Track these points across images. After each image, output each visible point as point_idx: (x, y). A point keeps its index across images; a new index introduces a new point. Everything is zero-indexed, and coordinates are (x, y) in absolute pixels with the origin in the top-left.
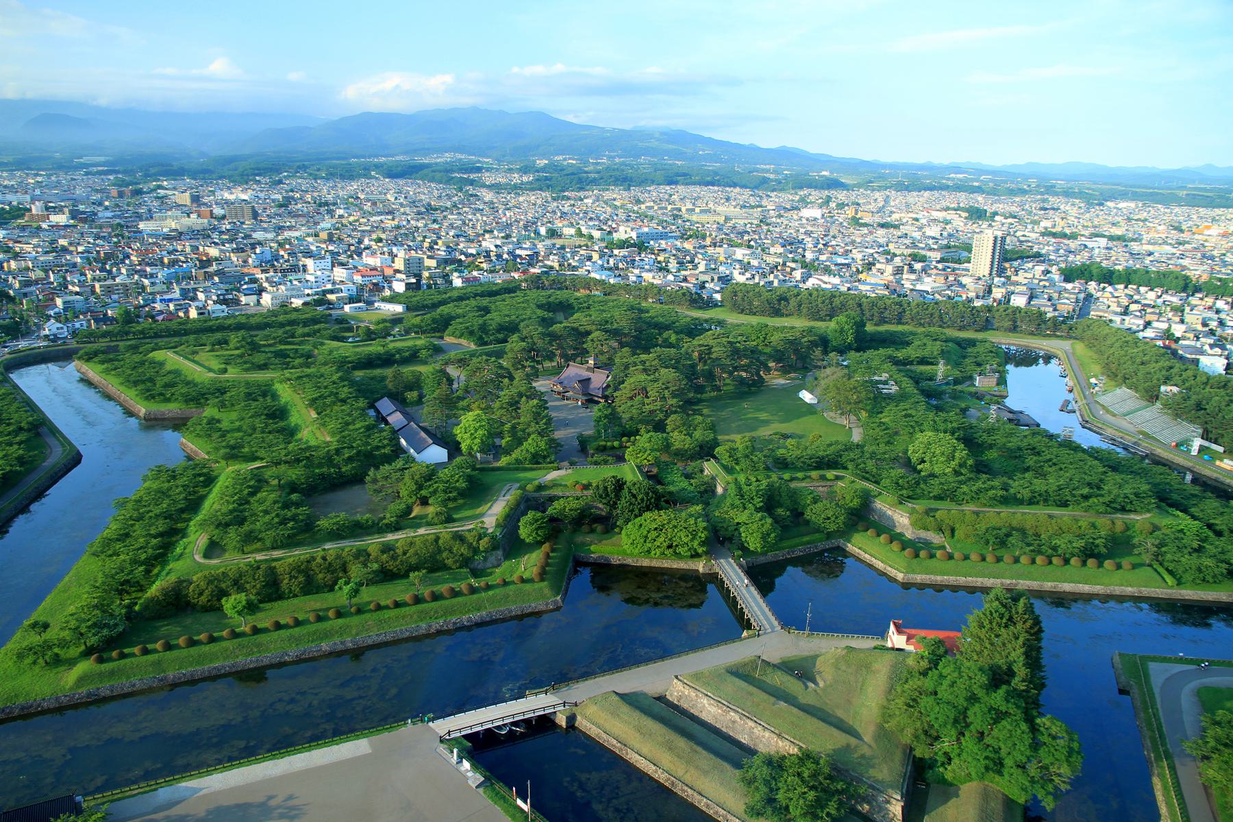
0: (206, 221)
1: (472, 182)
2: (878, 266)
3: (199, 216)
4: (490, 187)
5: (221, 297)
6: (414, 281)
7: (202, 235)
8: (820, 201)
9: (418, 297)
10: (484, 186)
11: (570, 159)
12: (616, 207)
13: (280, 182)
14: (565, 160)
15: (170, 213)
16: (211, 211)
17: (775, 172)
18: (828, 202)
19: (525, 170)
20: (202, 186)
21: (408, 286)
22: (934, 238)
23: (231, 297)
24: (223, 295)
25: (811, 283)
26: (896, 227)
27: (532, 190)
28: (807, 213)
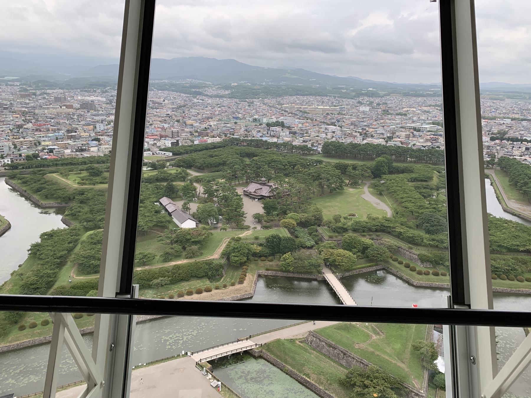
0: (70, 110)
1: (200, 94)
2: (397, 134)
3: (66, 108)
4: (211, 97)
5: (80, 148)
6: (176, 141)
7: (69, 117)
8: (368, 103)
9: (176, 149)
10: (207, 95)
11: (247, 83)
12: (270, 106)
13: (106, 91)
14: (245, 83)
15: (51, 106)
16: (72, 105)
17: (346, 89)
18: (372, 103)
19: (226, 88)
20: (67, 93)
21: (172, 144)
22: (424, 120)
23: (84, 148)
24: (81, 147)
25: (365, 142)
26: (405, 115)
27: (229, 98)
28: (362, 108)
